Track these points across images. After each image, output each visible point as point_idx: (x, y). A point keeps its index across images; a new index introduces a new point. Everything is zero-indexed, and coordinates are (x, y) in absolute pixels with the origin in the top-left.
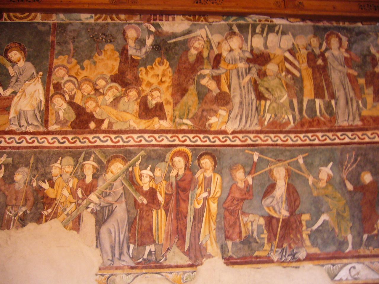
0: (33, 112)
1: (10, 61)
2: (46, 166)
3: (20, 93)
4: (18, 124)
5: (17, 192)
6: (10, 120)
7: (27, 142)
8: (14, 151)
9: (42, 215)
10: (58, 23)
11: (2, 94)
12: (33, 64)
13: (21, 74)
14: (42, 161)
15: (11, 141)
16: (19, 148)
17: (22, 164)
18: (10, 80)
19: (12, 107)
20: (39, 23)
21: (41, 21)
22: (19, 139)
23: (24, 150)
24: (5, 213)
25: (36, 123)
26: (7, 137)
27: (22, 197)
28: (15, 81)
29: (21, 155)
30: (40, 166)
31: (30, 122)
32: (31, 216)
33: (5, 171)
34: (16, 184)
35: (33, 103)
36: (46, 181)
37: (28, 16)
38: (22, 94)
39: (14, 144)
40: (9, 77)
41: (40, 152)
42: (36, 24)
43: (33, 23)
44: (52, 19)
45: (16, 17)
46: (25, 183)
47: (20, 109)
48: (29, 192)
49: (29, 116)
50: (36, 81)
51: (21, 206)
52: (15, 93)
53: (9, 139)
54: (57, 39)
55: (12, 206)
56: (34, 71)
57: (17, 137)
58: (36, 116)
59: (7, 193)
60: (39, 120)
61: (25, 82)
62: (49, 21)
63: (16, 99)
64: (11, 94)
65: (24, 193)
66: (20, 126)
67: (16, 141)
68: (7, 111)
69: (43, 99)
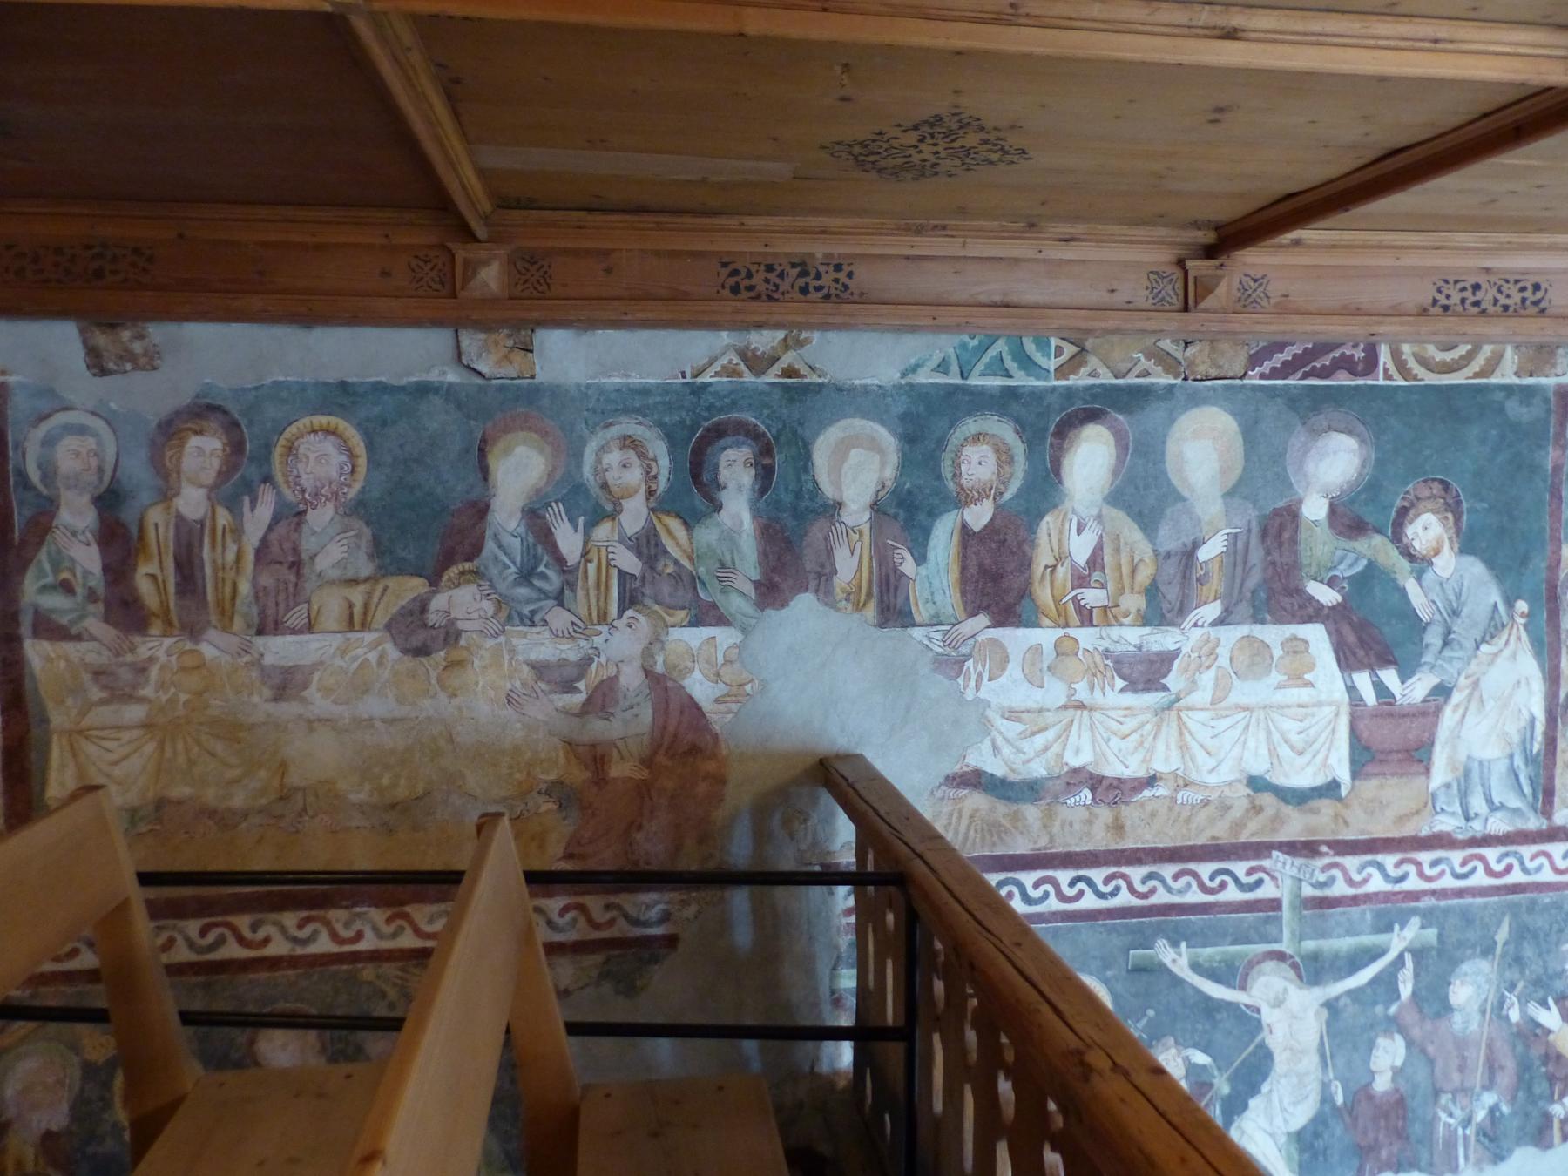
0: (1507, 761)
2: (1549, 952)
3: (1461, 690)
5: (1461, 1044)
6: (1434, 796)
7: (1490, 872)
8: (1443, 903)
9: (1548, 1118)
11: (1398, 696)
12: (1490, 564)
14: (1535, 936)
16: (1460, 893)
17: (1473, 947)
18: (1422, 640)
19: (1438, 748)
20: (1509, 390)
21: (1517, 381)
22: (1464, 864)
23: (1479, 900)
24: (1436, 1118)
26: (1425, 857)
27: (1479, 1058)
28: (1439, 643)
29: (1467, 917)
30: (1529, 952)
31: (1497, 802)
32: (1516, 1123)
33: (1416, 975)
34: (1457, 1018)
35: (1507, 728)
36: (1551, 1002)
37: (1469, 357)
38: (1471, 694)
39: (1448, 882)
40: (1418, 627)
41: (1532, 907)
42: (1499, 396)
43: (1486, 387)
46: (1483, 1012)
47: (1469, 757)
48: (1498, 1044)
50: (1513, 638)
51: (1478, 1089)
52: (1442, 692)
53: (1435, 863)
55: (1454, 1093)
56: (1495, 596)
57: (1456, 856)
59: (1430, 1049)
60: (1527, 789)
61: (1478, 648)
62: (1543, 381)
63: (1449, 718)
65: (1483, 1046)
66: (1468, 819)
68: (1420, 761)
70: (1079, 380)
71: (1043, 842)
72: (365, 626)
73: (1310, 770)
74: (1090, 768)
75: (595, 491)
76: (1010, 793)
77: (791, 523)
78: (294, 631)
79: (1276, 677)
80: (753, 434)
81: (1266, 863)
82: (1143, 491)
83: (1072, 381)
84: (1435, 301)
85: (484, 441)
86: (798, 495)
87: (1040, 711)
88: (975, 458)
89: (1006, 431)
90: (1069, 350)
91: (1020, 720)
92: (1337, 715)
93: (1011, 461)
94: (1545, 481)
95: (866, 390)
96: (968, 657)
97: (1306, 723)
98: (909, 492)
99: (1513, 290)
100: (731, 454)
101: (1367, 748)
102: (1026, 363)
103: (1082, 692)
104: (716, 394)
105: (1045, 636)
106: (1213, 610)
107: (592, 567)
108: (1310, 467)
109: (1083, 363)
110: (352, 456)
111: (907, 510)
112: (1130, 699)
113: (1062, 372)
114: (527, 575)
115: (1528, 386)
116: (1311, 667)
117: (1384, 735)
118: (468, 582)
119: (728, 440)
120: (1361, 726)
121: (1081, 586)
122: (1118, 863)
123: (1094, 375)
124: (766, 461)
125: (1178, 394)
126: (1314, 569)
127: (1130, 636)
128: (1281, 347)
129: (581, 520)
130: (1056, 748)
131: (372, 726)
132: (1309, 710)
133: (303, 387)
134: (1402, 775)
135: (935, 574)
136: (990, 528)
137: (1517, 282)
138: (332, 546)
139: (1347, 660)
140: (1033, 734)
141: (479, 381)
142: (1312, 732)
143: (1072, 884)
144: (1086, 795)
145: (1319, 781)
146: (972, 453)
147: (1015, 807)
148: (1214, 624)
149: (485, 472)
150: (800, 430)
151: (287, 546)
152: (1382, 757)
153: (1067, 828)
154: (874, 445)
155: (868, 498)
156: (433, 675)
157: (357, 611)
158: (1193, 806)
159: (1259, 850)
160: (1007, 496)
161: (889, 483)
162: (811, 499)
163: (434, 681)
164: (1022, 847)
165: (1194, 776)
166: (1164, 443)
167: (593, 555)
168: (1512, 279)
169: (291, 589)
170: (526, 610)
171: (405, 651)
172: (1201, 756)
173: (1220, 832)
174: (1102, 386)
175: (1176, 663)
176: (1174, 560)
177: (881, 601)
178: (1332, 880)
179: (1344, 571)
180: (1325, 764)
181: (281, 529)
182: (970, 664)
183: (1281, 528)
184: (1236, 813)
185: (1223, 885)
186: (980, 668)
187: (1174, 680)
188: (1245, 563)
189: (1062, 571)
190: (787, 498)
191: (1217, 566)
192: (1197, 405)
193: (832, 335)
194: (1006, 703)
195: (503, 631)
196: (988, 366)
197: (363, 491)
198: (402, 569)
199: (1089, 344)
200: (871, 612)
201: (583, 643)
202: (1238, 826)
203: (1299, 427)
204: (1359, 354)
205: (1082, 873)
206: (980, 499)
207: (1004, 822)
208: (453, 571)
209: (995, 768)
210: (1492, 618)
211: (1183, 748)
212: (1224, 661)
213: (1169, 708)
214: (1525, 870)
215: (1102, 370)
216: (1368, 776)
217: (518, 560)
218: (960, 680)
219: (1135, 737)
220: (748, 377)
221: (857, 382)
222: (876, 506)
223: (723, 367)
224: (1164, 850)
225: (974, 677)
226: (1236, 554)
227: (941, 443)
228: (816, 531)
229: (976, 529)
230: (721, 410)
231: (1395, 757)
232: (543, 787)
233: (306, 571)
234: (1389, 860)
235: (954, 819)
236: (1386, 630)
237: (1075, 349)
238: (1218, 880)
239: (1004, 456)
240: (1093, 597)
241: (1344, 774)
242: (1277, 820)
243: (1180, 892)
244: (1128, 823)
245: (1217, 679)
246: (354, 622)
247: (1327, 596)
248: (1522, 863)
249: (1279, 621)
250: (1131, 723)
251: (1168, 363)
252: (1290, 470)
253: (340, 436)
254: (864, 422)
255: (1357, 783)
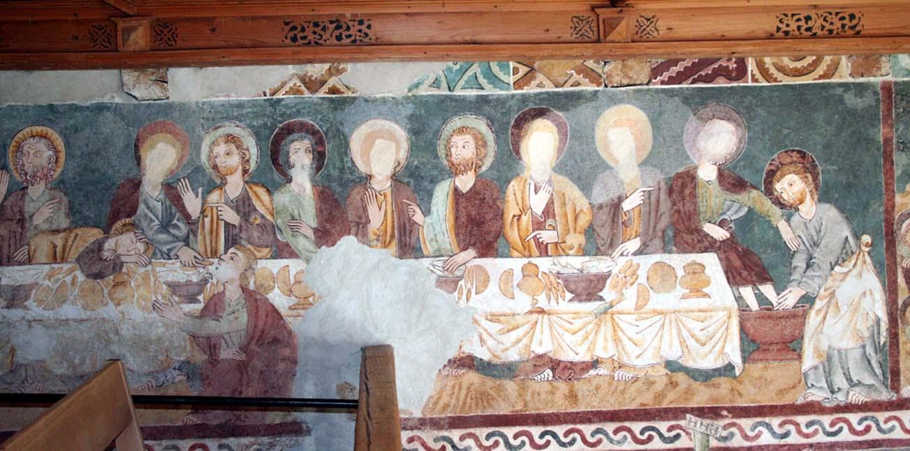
0: (860, 350)
1: (779, 203)
3: (821, 299)
4: (825, 386)
6: (806, 375)
7: (853, 431)
10: (896, 83)
11: (775, 304)
12: (842, 210)
13: (816, 244)
15: (812, 429)
18: (791, 263)
19: (806, 340)
20: (846, 86)
21: (851, 80)
22: (832, 424)
25: (869, 380)
26: (802, 420)
28: (804, 266)
31: (855, 379)
37: (815, 65)
38: (829, 302)
42: (840, 91)
44: (879, 73)
45: (781, 69)
47: (829, 347)
49: (851, 364)
50: (859, 262)
52: (808, 300)
53: (809, 425)
54: (899, 132)
56: (846, 232)
57: (826, 420)
58: (869, 362)
60: (878, 371)
61: (832, 269)
62: (872, 79)
63: (813, 320)
64: (798, 302)
66: (833, 392)
67: (824, 429)
68: (794, 350)
69: (882, 313)
70: (531, 90)
71: (519, 407)
72: (63, 260)
73: (712, 357)
74: (550, 355)
75: (210, 171)
76: (495, 373)
77: (339, 190)
78: (20, 264)
79: (680, 291)
80: (313, 132)
81: (682, 423)
82: (580, 163)
83: (526, 90)
84: (778, 29)
85: (138, 140)
86: (342, 170)
87: (514, 315)
88: (460, 144)
89: (481, 125)
90: (523, 70)
91: (499, 321)
92: (729, 317)
93: (485, 145)
94: (878, 150)
95: (384, 101)
96: (461, 278)
97: (706, 323)
98: (417, 167)
99: (836, 20)
100: (296, 145)
101: (753, 341)
102: (494, 79)
103: (543, 302)
104: (286, 106)
105: (516, 264)
106: (634, 244)
107: (207, 220)
108: (701, 144)
109: (533, 78)
110: (56, 151)
111: (415, 180)
112: (576, 306)
113: (518, 85)
114: (165, 226)
115: (860, 84)
116: (708, 283)
117: (768, 331)
118: (128, 230)
119: (296, 135)
120: (748, 325)
121: (539, 229)
122: (574, 422)
123: (541, 85)
124: (320, 149)
125: (600, 96)
126: (709, 215)
127: (574, 263)
128: (675, 62)
129: (200, 190)
130: (525, 341)
131: (68, 324)
132: (708, 314)
133: (26, 109)
134: (781, 360)
135: (437, 221)
136: (474, 191)
137: (837, 14)
138: (43, 208)
139: (734, 277)
140: (509, 331)
141: (135, 101)
142: (711, 329)
143: (542, 436)
144: (548, 373)
145: (720, 364)
146: (458, 140)
147: (498, 382)
148: (635, 254)
149: (138, 160)
150: (341, 128)
151: (16, 209)
152: (766, 347)
153: (536, 396)
154: (391, 137)
155: (389, 172)
156: (106, 291)
157: (59, 250)
158: (626, 382)
159: (678, 413)
160: (484, 168)
161: (403, 162)
162: (351, 173)
163: (106, 295)
164: (503, 409)
165: (625, 360)
166: (593, 130)
167: (208, 212)
168: (833, 11)
169: (18, 236)
170: (165, 249)
171: (88, 276)
172: (629, 346)
173: (646, 399)
174: (547, 93)
175: (609, 281)
176: (605, 210)
177: (400, 241)
178: (732, 435)
179: (731, 215)
180: (722, 352)
181: (12, 199)
182: (462, 283)
183: (683, 186)
184: (659, 387)
185: (650, 438)
186: (469, 285)
187: (608, 293)
188: (657, 211)
189: (524, 218)
190: (335, 173)
191: (636, 214)
192: (615, 104)
193: (359, 65)
194: (489, 310)
195: (150, 263)
196: (467, 82)
197: (63, 173)
198: (87, 223)
199: (536, 65)
200: (394, 247)
201: (201, 270)
202: (660, 396)
203: (692, 117)
204: (732, 66)
205: (549, 428)
206: (466, 171)
207: (491, 392)
208: (119, 224)
209: (483, 354)
210: (844, 248)
211: (617, 340)
212: (642, 279)
213: (605, 313)
214: (880, 430)
215: (547, 82)
216: (755, 361)
217: (160, 217)
218: (456, 294)
219: (582, 333)
220: (307, 94)
221: (378, 96)
222: (395, 178)
223: (291, 88)
224: (607, 412)
225: (465, 292)
226: (651, 206)
227: (437, 133)
228: (356, 195)
229: (464, 191)
230: (290, 116)
231: (775, 347)
232: (177, 365)
233: (27, 225)
234: (775, 422)
235: (456, 390)
236: (763, 256)
237: (528, 69)
238: (647, 434)
239: (481, 142)
240: (547, 236)
241: (737, 359)
242: (689, 392)
243: (619, 442)
244: (580, 394)
245: (638, 292)
246: (56, 257)
247: (719, 234)
248: (878, 425)
249: (684, 251)
250: (578, 323)
251: (595, 78)
252: (687, 146)
253: (49, 139)
254: (384, 122)
255: (747, 365)
